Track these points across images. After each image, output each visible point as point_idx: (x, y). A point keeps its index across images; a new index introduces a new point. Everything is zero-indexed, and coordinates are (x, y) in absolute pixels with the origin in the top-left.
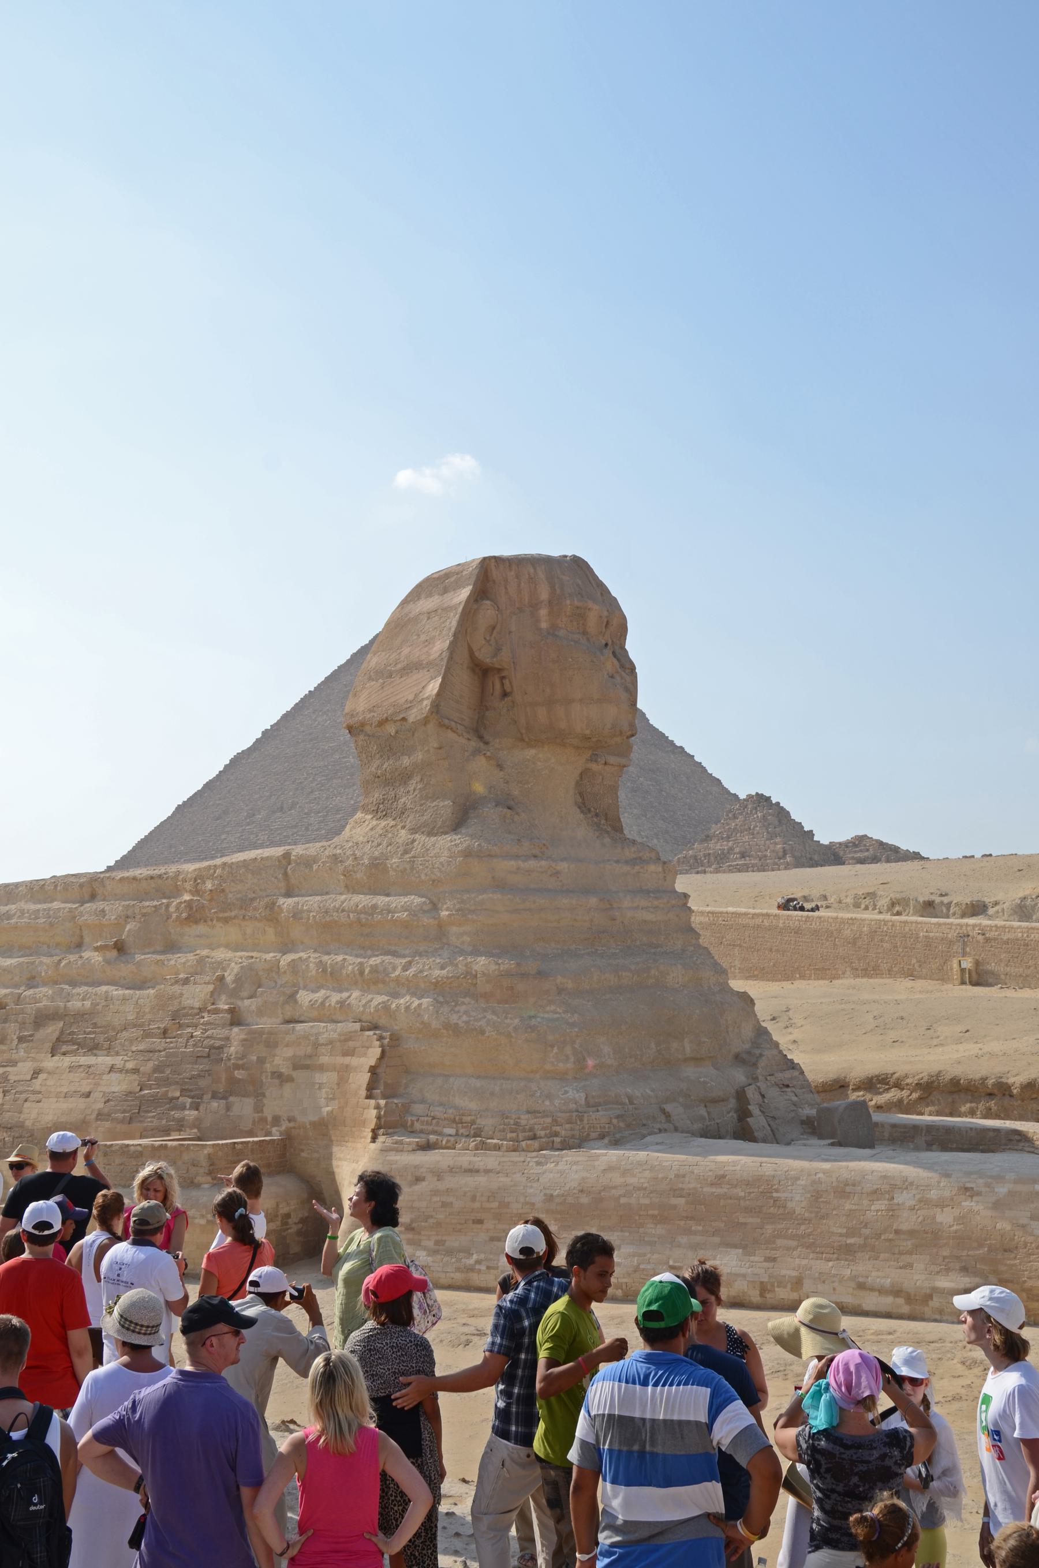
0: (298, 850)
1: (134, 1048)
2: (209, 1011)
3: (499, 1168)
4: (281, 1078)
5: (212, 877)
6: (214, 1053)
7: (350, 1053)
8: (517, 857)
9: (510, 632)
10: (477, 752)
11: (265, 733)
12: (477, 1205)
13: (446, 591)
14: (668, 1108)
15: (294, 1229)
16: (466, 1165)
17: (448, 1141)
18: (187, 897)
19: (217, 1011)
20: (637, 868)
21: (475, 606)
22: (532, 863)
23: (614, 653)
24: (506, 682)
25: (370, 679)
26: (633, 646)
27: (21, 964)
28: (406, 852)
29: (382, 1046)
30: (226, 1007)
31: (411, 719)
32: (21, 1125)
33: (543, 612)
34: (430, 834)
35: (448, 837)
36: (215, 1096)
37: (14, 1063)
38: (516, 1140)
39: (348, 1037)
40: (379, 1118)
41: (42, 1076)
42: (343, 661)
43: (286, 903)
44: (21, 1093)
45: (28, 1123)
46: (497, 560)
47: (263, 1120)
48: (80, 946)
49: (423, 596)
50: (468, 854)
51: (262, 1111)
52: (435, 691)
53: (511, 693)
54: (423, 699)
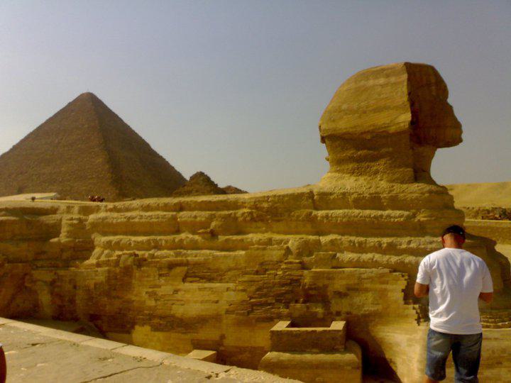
2: (285, 263)
4: (340, 295)
5: (267, 201)
6: (295, 282)
18: (246, 210)
27: (149, 240)
30: (297, 261)
31: (391, 132)
32: (173, 316)
33: (433, 88)
34: (402, 183)
36: (297, 302)
37: (159, 286)
39: (382, 275)
40: (417, 313)
43: (321, 213)
44: (168, 300)
47: (331, 313)
48: (178, 232)
51: (329, 309)
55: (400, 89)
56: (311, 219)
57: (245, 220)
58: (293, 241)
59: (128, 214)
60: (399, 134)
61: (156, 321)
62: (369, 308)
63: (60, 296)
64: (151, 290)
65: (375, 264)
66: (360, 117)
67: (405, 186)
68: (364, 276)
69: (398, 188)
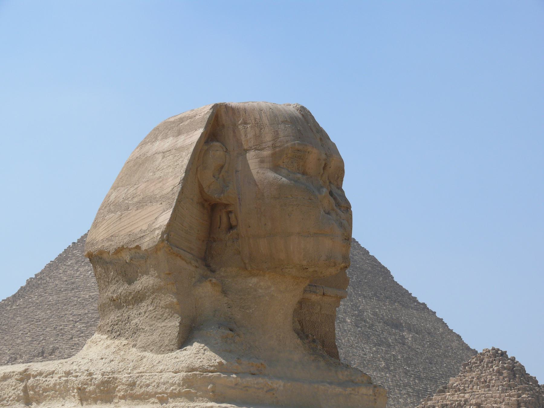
0: (36, 367)
9: (237, 171)
10: (204, 278)
11: (29, 282)
13: (179, 133)
20: (349, 390)
21: (206, 147)
22: (250, 380)
23: (331, 193)
24: (232, 216)
25: (110, 211)
26: (349, 187)
28: (135, 368)
31: (144, 247)
33: (267, 153)
35: (174, 354)
49: (160, 138)
52: (166, 222)
53: (236, 226)
55: (179, 162)
60: (156, 249)
67: (160, 356)
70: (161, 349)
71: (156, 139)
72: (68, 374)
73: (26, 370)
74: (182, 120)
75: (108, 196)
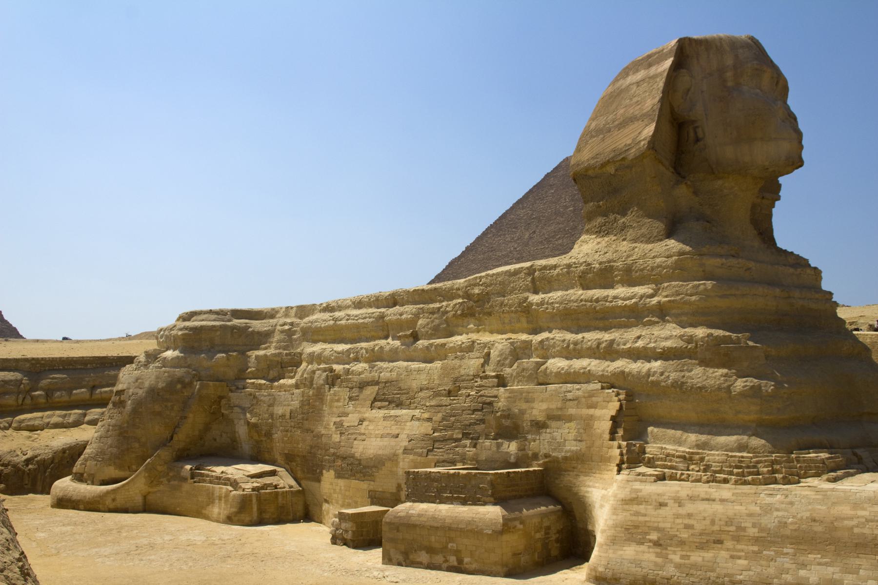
1: (428, 404)
2: (481, 378)
3: (734, 498)
4: (539, 426)
5: (479, 285)
7: (593, 406)
8: (721, 256)
11: (467, 248)
12: (716, 528)
13: (650, 65)
14: (858, 451)
15: (554, 537)
16: (703, 495)
17: (682, 474)
19: (486, 377)
20: (799, 270)
22: (733, 261)
25: (592, 137)
28: (628, 256)
29: (619, 400)
30: (494, 374)
31: (631, 157)
32: (353, 456)
33: (729, 74)
35: (664, 243)
37: (346, 415)
38: (742, 475)
39: (591, 394)
40: (621, 454)
41: (365, 423)
42: (508, 208)
43: (535, 298)
44: (352, 434)
45: (357, 455)
46: (690, 40)
50: (681, 253)
52: (651, 133)
54: (640, 141)
55: (655, 86)
56: (526, 309)
57: (454, 315)
58: (499, 342)
59: (337, 314)
60: (641, 157)
61: (339, 463)
62: (572, 447)
63: (255, 426)
64: (338, 419)
65: (585, 377)
66: (603, 140)
68: (570, 396)
69: (642, 248)
70: (649, 241)
71: (627, 75)
72: (569, 266)
73: (532, 266)
74: (649, 56)
75: (588, 126)
